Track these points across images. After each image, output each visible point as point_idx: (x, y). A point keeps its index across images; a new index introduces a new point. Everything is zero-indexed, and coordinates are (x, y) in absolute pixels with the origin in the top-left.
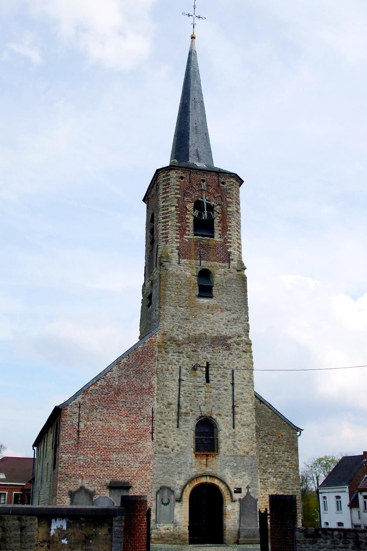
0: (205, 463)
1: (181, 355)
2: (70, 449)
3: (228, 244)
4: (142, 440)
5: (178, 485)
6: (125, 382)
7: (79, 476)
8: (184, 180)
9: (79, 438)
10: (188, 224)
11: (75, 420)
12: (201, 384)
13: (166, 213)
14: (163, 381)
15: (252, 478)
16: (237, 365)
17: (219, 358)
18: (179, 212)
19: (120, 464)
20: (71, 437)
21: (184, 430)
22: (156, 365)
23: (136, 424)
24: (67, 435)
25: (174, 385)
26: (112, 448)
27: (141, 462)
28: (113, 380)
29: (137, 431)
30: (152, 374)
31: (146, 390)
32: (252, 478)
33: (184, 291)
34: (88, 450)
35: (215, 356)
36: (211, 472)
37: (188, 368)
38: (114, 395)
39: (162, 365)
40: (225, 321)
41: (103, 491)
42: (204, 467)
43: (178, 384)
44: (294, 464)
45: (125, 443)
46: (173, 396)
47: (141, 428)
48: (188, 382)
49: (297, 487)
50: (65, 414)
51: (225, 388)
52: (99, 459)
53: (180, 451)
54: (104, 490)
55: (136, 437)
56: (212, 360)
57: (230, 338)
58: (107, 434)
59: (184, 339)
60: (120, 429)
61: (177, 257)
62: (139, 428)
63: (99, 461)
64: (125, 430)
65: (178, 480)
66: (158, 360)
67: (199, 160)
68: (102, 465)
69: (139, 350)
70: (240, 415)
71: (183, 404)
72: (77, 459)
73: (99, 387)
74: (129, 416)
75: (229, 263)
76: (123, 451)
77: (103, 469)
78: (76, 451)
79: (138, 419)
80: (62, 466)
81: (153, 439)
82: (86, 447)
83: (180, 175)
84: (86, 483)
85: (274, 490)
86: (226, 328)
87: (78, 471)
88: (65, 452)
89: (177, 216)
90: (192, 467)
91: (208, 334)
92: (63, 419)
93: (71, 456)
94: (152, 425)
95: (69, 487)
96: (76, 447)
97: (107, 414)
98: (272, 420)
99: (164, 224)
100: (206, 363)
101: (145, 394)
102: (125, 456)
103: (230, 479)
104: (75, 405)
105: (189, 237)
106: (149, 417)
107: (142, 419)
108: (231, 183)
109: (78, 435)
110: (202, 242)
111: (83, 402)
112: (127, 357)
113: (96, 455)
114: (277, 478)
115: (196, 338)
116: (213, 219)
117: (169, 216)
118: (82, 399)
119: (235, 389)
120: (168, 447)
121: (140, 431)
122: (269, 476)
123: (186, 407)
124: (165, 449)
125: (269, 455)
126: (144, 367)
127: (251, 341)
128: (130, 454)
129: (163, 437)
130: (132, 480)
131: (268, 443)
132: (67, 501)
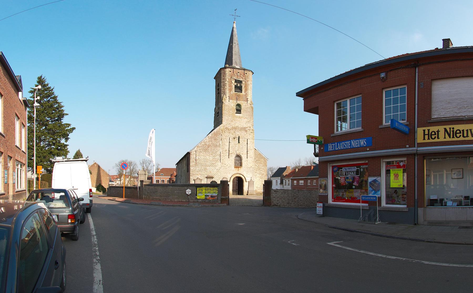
3: (247, 95)
10: (232, 88)
16: (249, 137)
30: (220, 140)
33: (231, 111)
40: (245, 122)
67: (237, 65)
83: (230, 70)
105: (233, 92)
123: (231, 151)
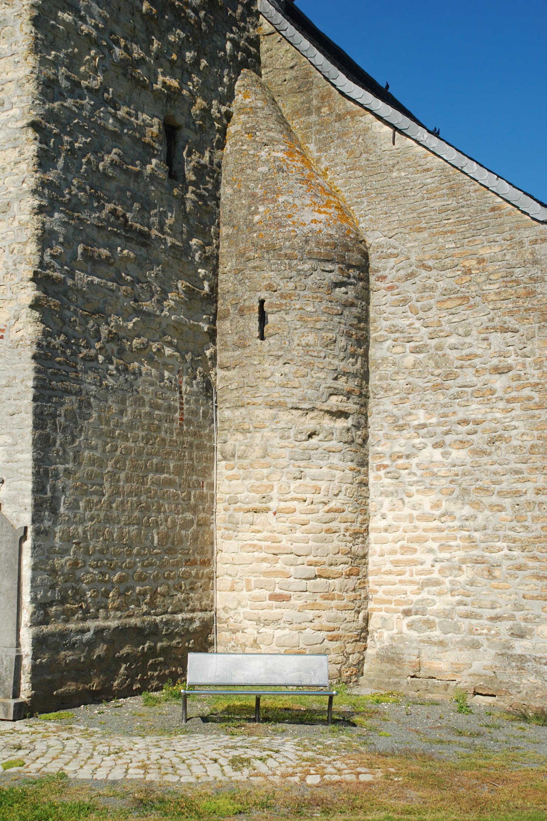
44: (531, 381)
85: (433, 497)
98: (437, 204)
114: (450, 450)
122: (417, 441)
125: (421, 356)
131: (419, 304)
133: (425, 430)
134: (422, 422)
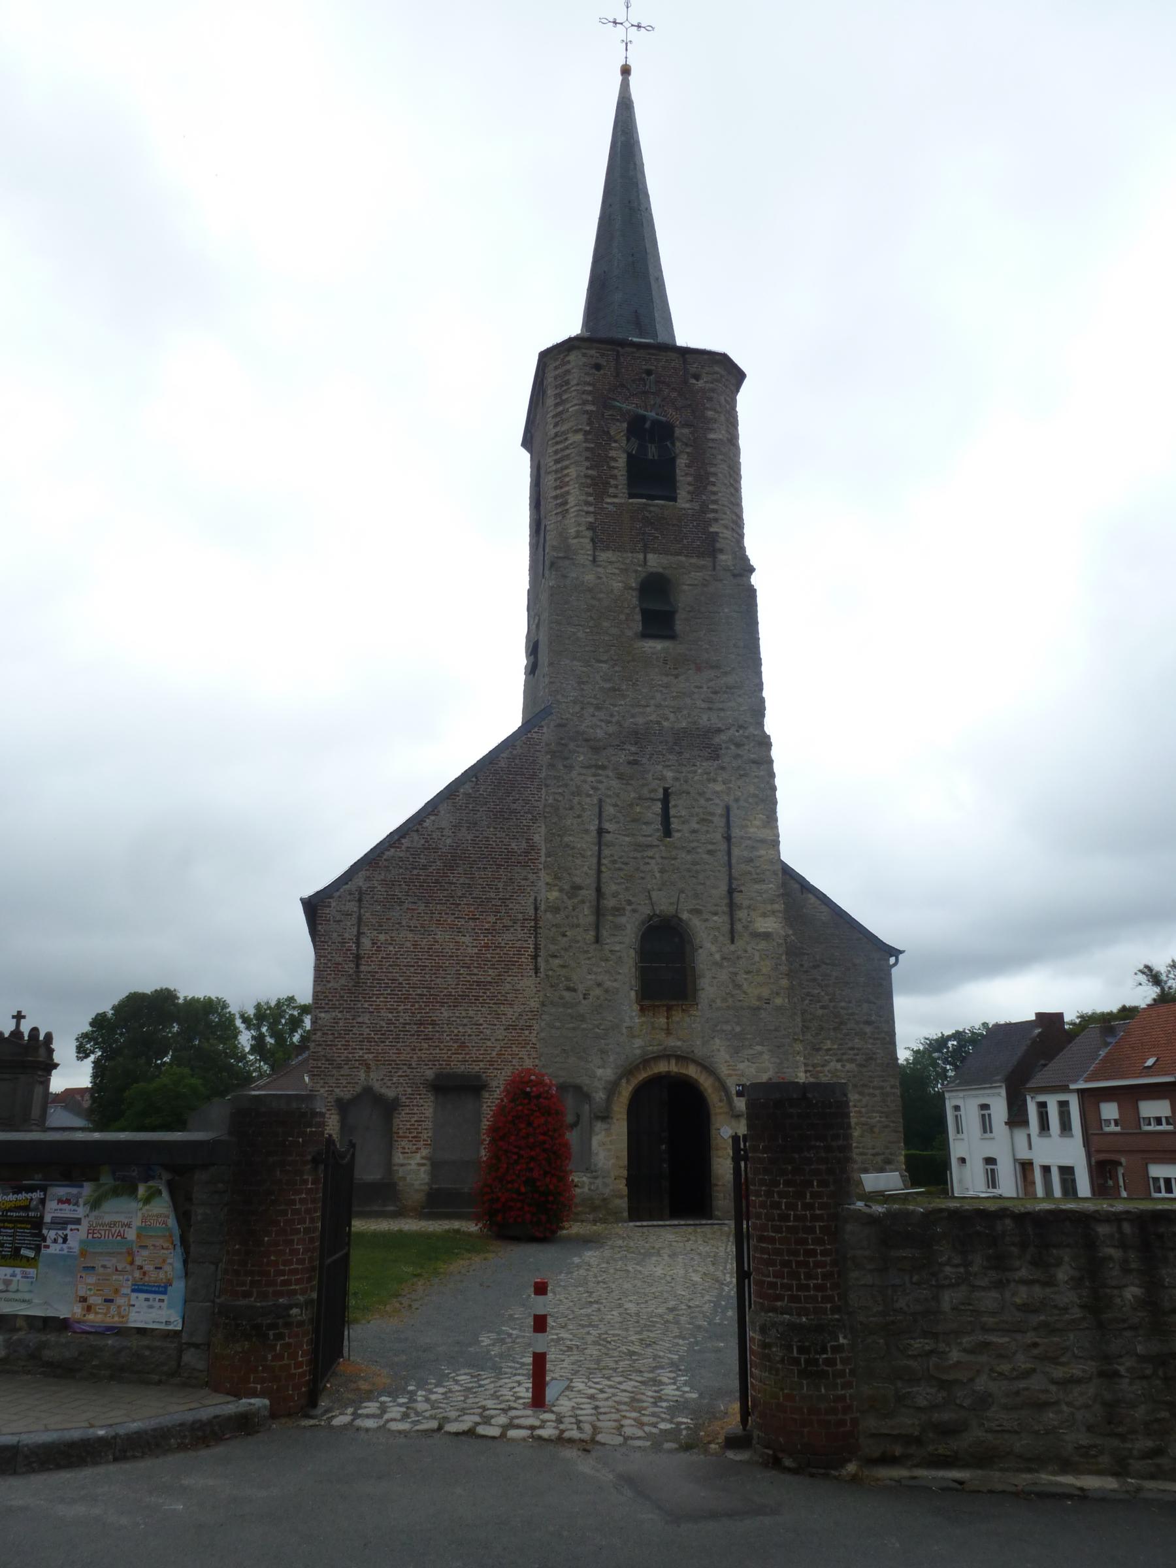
0: (665, 1027)
1: (600, 772)
2: (338, 998)
3: (711, 515)
4: (510, 974)
5: (599, 1080)
6: (469, 838)
7: (359, 1064)
8: (602, 372)
9: (358, 972)
10: (616, 471)
11: (348, 930)
12: (650, 839)
13: (562, 450)
14: (559, 835)
15: (778, 1061)
17: (693, 778)
18: (592, 445)
19: (459, 1032)
20: (340, 971)
21: (613, 948)
22: (543, 797)
23: (495, 936)
24: (329, 965)
25: (585, 843)
26: (438, 995)
27: (509, 1025)
28: (439, 834)
29: (498, 954)
30: (534, 820)
31: (519, 856)
32: (778, 1061)
33: (606, 624)
34: (381, 1001)
35: (683, 774)
36: (679, 1047)
37: (619, 803)
38: (443, 870)
39: (557, 797)
41: (418, 1097)
42: (661, 1036)
43: (596, 840)
45: (469, 981)
46: (585, 869)
47: (507, 946)
48: (618, 836)
49: (893, 1083)
50: (326, 917)
51: (710, 847)
52: (408, 1021)
53: (602, 998)
54: (420, 1095)
55: (496, 966)
56: (677, 784)
57: (719, 731)
58: (427, 961)
59: (607, 737)
60: (459, 949)
61: (590, 546)
62: (503, 945)
63: (407, 1026)
64: (470, 951)
65: (599, 1068)
66: (547, 786)
68: (414, 1035)
69: (502, 764)
70: (746, 911)
71: (610, 888)
72: (355, 1021)
73: (407, 851)
74: (479, 919)
75: (715, 557)
76: (466, 1001)
77: (416, 1044)
78: (352, 1003)
79: (501, 925)
80: (319, 1041)
81: (537, 970)
82: (375, 992)
84: (378, 1080)
86: (710, 709)
87: (358, 1051)
88: (327, 1006)
89: (588, 454)
90: (634, 1037)
91: (665, 724)
92: (319, 929)
93: (340, 1015)
94: (535, 937)
95: (335, 1089)
96: (352, 993)
97: (427, 913)
99: (559, 475)
100: (661, 791)
101: (516, 866)
102: (471, 1013)
103: (725, 1065)
104: (350, 894)
105: (616, 500)
106: (527, 920)
107: (510, 923)
108: (715, 376)
109: (358, 966)
110: (647, 511)
111: (369, 887)
112: (474, 779)
113: (400, 1012)
115: (636, 733)
116: (673, 460)
117: (569, 455)
118: (365, 880)
119: (736, 852)
120: (574, 990)
121: (505, 954)
122: (827, 1058)
124: (566, 994)
125: (826, 1011)
126: (515, 803)
127: (769, 737)
128: (482, 1007)
129: (563, 966)
130: (489, 1069)
132: (330, 1123)
133: (831, 1052)
134: (829, 1047)
